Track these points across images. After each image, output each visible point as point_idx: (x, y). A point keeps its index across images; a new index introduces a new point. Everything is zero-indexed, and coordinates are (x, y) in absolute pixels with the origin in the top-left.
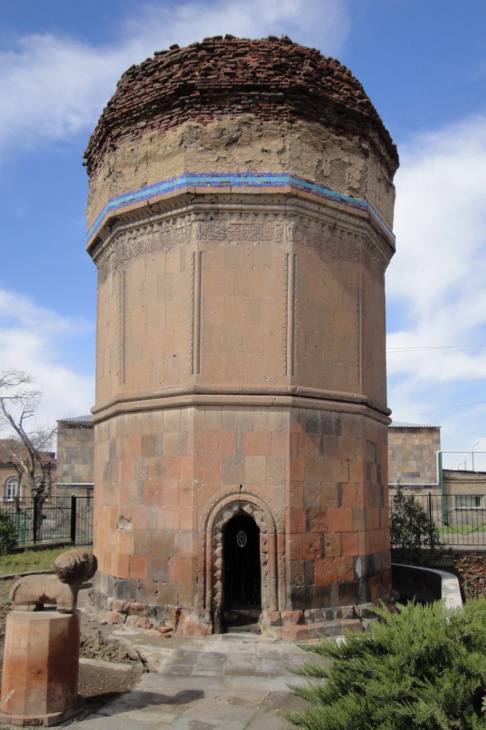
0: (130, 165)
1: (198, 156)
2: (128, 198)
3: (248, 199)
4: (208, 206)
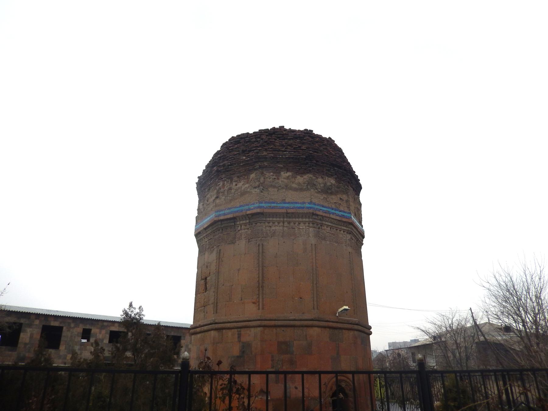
0: (274, 187)
1: (316, 195)
2: (273, 205)
3: (335, 222)
4: (319, 222)
